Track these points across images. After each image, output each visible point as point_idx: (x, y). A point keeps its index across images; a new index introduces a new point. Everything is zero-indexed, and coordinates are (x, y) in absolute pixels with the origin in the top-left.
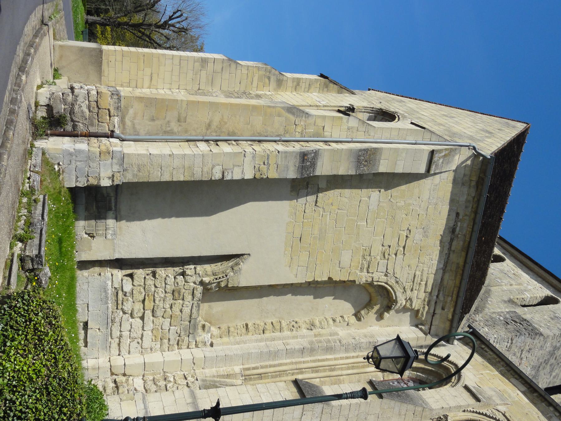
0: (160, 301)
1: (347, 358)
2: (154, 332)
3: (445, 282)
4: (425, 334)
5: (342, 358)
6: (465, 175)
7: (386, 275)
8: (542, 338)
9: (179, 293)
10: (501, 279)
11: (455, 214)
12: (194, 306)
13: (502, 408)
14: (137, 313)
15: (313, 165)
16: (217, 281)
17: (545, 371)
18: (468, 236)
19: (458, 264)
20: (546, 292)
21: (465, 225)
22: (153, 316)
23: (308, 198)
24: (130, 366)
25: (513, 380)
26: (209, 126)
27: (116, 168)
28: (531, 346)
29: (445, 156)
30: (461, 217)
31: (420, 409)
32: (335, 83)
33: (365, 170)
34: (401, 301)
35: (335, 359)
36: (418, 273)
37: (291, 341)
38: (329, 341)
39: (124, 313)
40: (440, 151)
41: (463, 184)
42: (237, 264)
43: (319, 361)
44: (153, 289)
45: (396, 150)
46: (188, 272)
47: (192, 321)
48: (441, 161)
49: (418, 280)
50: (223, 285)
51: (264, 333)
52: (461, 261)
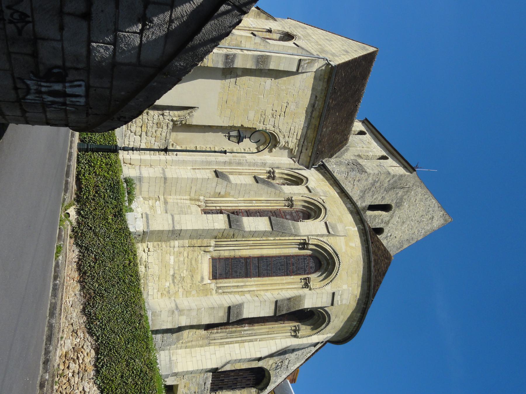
1: (249, 169)
3: (308, 135)
4: (295, 162)
5: (246, 169)
6: (321, 75)
7: (274, 127)
8: (366, 174)
9: (160, 124)
10: (358, 144)
11: (314, 97)
13: (323, 198)
15: (233, 61)
17: (369, 194)
18: (321, 110)
19: (315, 125)
20: (384, 153)
21: (320, 103)
23: (232, 80)
24: (133, 159)
25: (335, 187)
28: (360, 178)
29: (308, 63)
30: (318, 99)
31: (278, 192)
32: (265, 13)
33: (262, 67)
34: (282, 143)
35: (243, 169)
36: (292, 128)
37: (219, 158)
38: (240, 160)
39: (131, 132)
40: (305, 60)
41: (320, 80)
42: (191, 112)
43: (234, 169)
44: (147, 121)
45: (280, 57)
46: (165, 114)
48: (306, 65)
49: (292, 131)
50: (183, 122)
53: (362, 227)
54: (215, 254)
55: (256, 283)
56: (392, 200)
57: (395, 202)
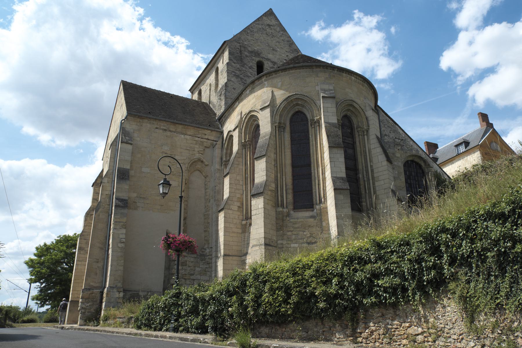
6: (137, 125)
21: (162, 124)
22: (193, 275)
25: (235, 106)
26: (101, 248)
27: (115, 290)
29: (125, 136)
30: (158, 127)
41: (142, 126)
48: (127, 138)
52: (181, 126)
53: (265, 78)
54: (291, 207)
55: (316, 168)
56: (253, 60)
57: (254, 58)
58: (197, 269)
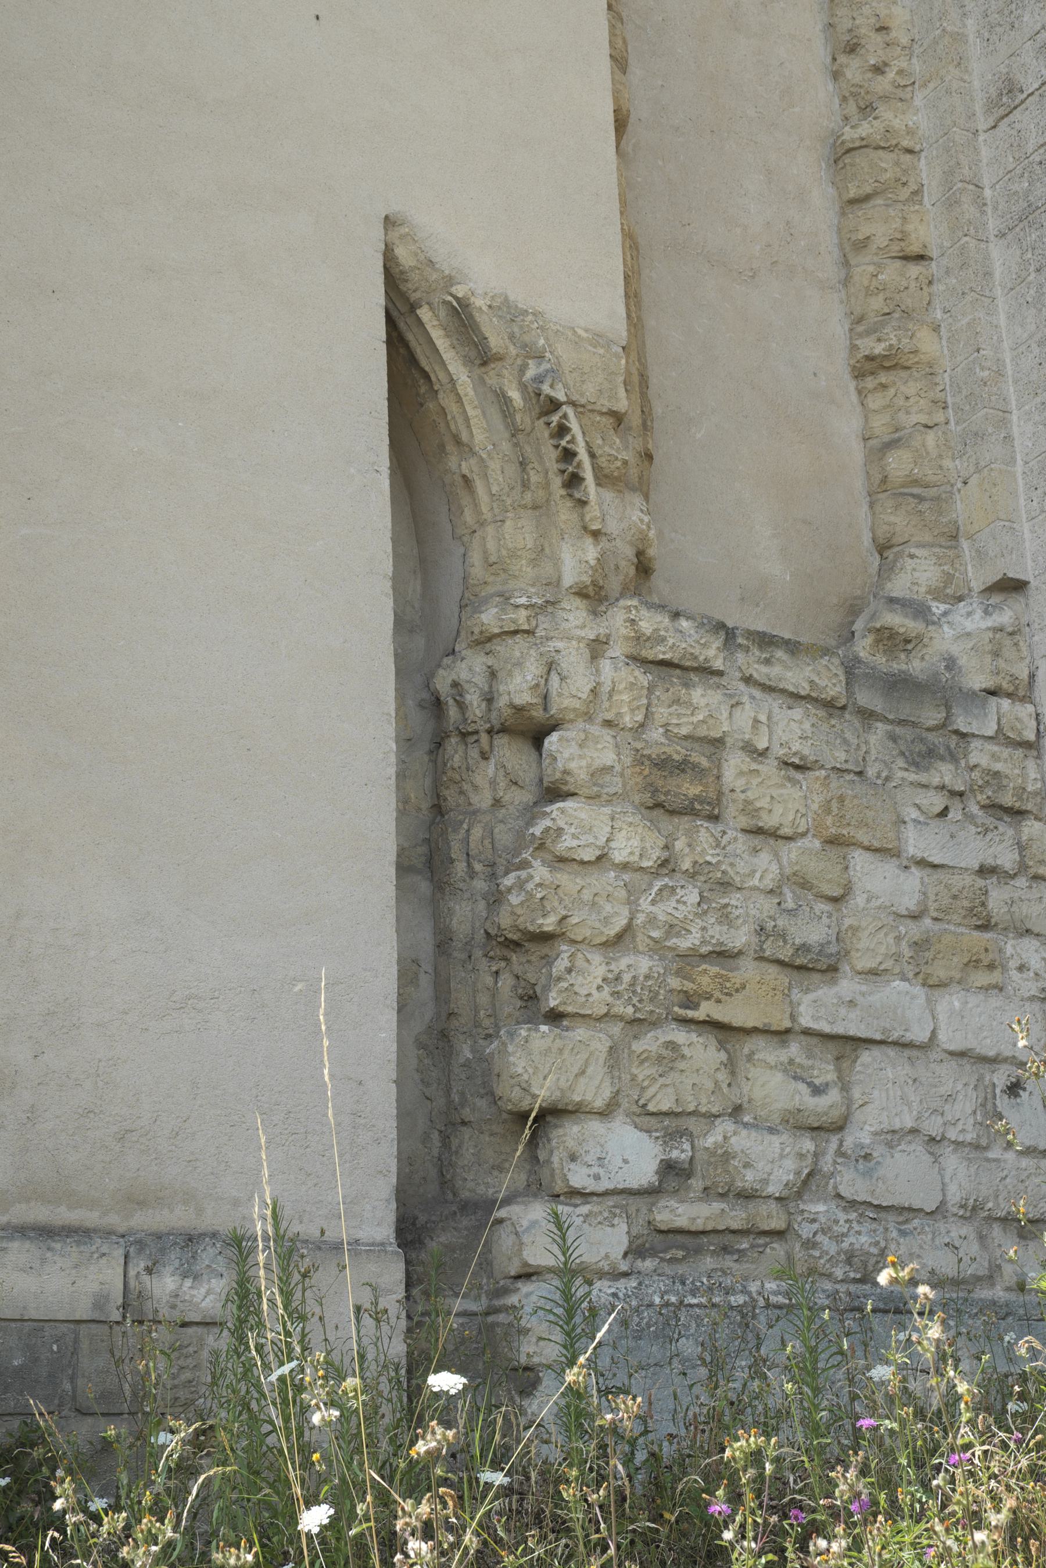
0: (725, 917)
2: (939, 971)
12: (759, 672)
14: (817, 1091)
16: (588, 475)
39: (809, 1182)
42: (461, 317)
47: (865, 698)
51: (921, 258)
58: (877, 882)
